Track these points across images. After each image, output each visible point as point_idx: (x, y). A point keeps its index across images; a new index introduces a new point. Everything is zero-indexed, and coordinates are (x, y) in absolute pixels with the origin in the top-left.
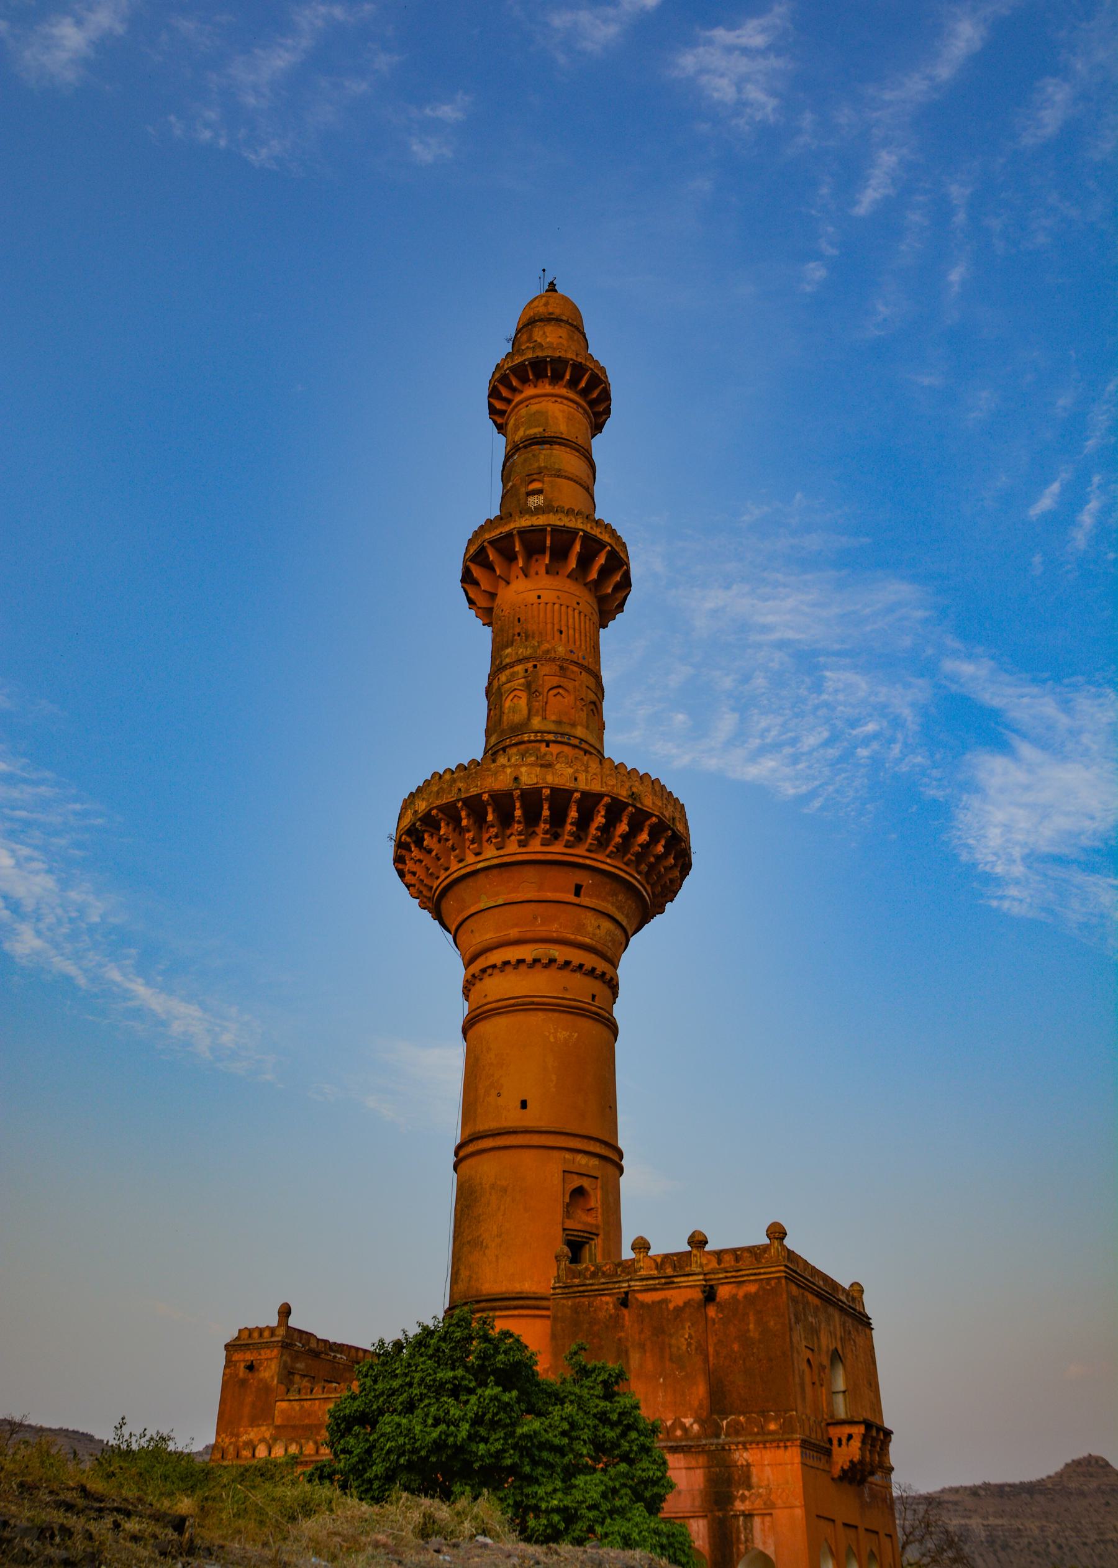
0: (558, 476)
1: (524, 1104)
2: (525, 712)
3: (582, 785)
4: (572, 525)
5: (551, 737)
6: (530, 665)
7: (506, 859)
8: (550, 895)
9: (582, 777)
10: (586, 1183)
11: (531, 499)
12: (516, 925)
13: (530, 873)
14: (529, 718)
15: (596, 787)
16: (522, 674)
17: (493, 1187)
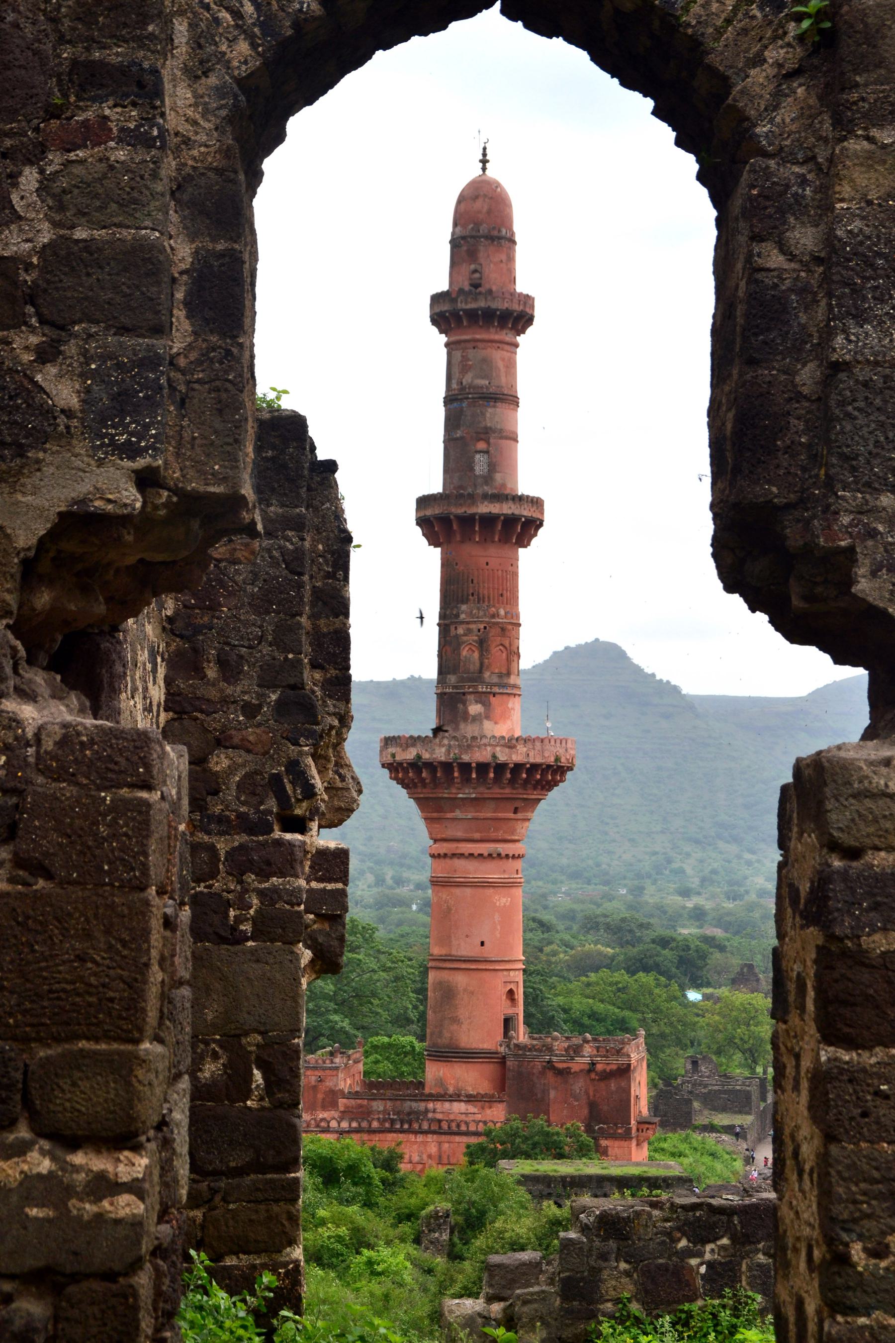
0: (501, 438)
1: (482, 944)
2: (478, 665)
3: (532, 760)
4: (517, 512)
5: (496, 690)
6: (482, 626)
7: (479, 796)
8: (500, 815)
9: (531, 754)
10: (512, 986)
11: (478, 456)
12: (477, 831)
13: (492, 805)
14: (481, 671)
15: (539, 760)
16: (476, 632)
17: (465, 990)
